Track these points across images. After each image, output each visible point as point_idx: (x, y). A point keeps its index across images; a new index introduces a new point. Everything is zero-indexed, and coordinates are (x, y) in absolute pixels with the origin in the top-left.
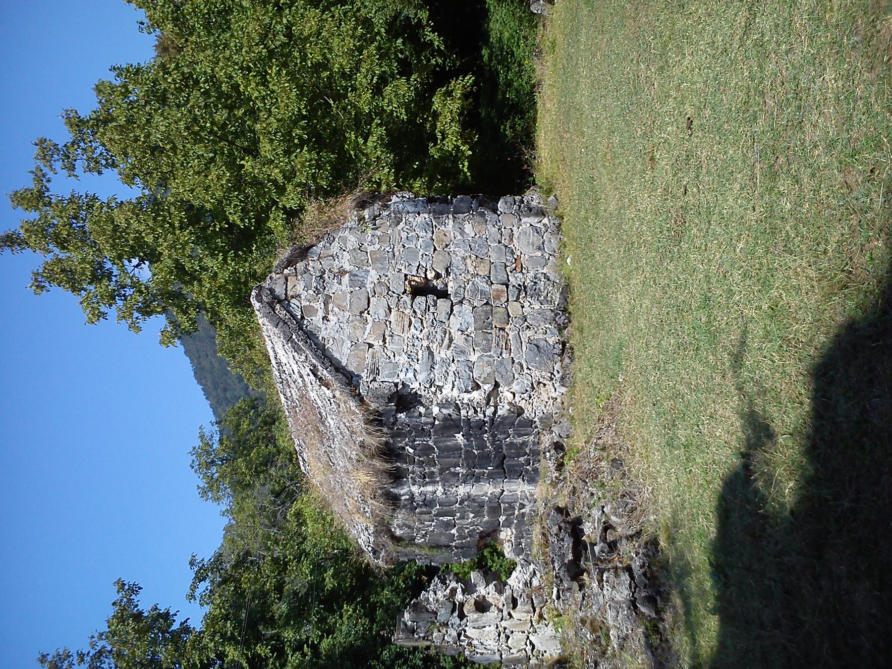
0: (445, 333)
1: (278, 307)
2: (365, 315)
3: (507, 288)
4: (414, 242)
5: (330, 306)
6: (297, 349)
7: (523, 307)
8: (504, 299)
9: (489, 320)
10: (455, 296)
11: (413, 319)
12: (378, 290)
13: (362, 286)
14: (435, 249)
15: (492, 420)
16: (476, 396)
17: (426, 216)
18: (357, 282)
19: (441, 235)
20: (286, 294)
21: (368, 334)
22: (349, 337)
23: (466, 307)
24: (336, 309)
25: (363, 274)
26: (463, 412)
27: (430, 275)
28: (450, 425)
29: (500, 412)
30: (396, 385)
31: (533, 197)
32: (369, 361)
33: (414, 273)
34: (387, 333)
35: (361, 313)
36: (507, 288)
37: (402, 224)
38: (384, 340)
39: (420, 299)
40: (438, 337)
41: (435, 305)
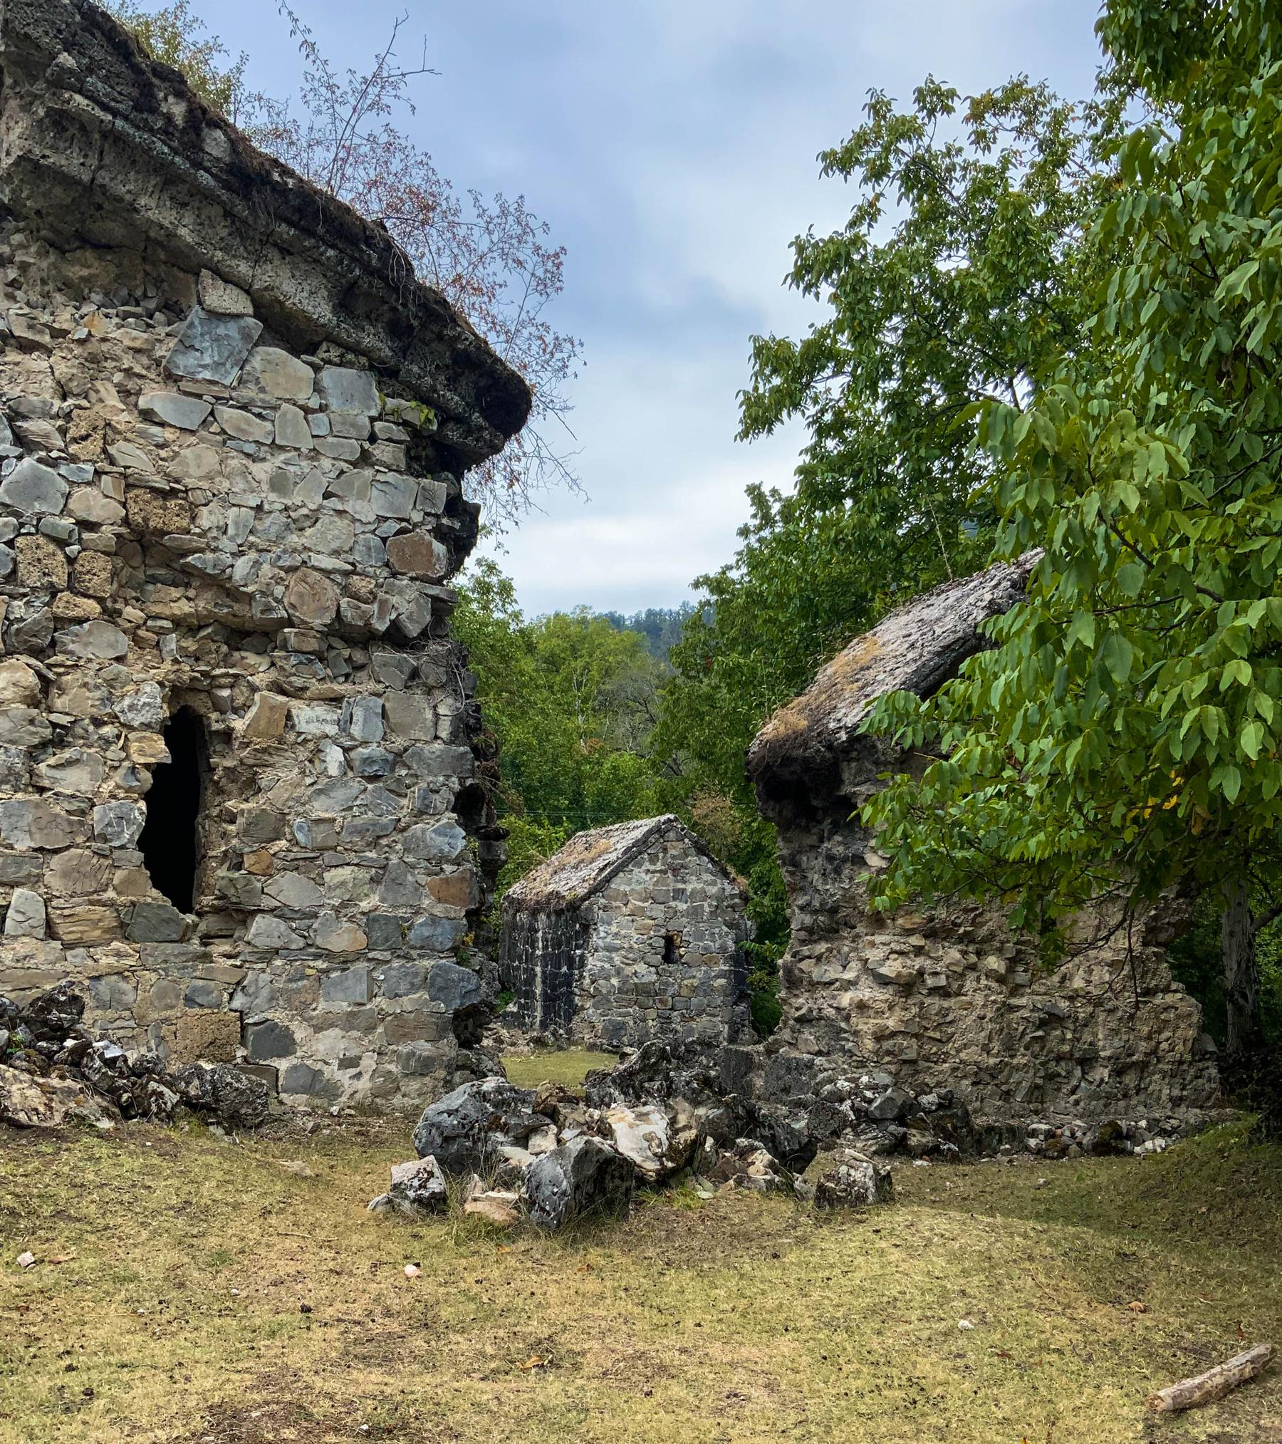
6: (625, 852)
9: (643, 993)
16: (587, 981)
18: (679, 894)
23: (655, 977)
28: (571, 963)
39: (662, 942)
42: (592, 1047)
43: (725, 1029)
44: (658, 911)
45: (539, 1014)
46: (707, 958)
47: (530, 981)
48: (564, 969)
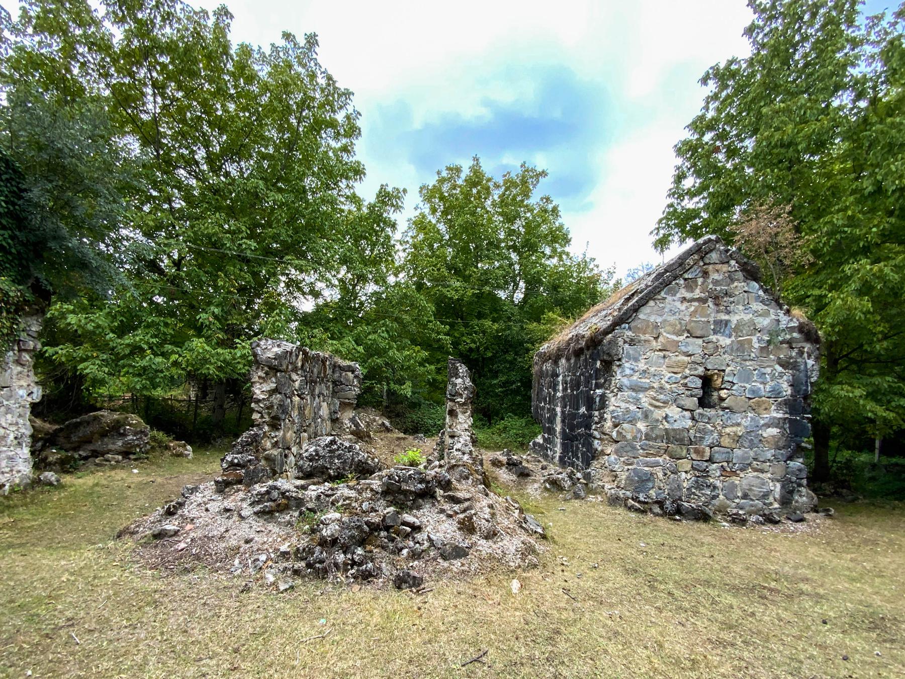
0: (664, 403)
1: (696, 257)
2: (686, 335)
3: (706, 461)
4: (760, 380)
5: (696, 304)
7: (686, 472)
8: (694, 456)
9: (675, 440)
10: (700, 414)
11: (680, 375)
12: (710, 346)
13: (715, 332)
14: (750, 399)
15: (591, 435)
16: (608, 424)
17: (789, 392)
18: (721, 326)
19: (766, 405)
20: (709, 264)
21: (667, 336)
22: (665, 321)
23: (689, 423)
24: (692, 309)
25: (727, 332)
26: (596, 413)
27: (723, 393)
28: (590, 403)
29: (596, 442)
30: (619, 360)
31: (804, 497)
32: (642, 337)
33: (726, 378)
34: (667, 353)
35: (688, 332)
36: (706, 461)
37: (779, 369)
38: (660, 350)
39: (699, 383)
40: (662, 397)
41: (692, 396)
42: (614, 501)
43: (777, 489)
44: (695, 346)
45: (558, 449)
46: (754, 404)
47: (552, 420)
48: (583, 410)
